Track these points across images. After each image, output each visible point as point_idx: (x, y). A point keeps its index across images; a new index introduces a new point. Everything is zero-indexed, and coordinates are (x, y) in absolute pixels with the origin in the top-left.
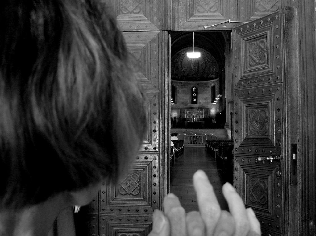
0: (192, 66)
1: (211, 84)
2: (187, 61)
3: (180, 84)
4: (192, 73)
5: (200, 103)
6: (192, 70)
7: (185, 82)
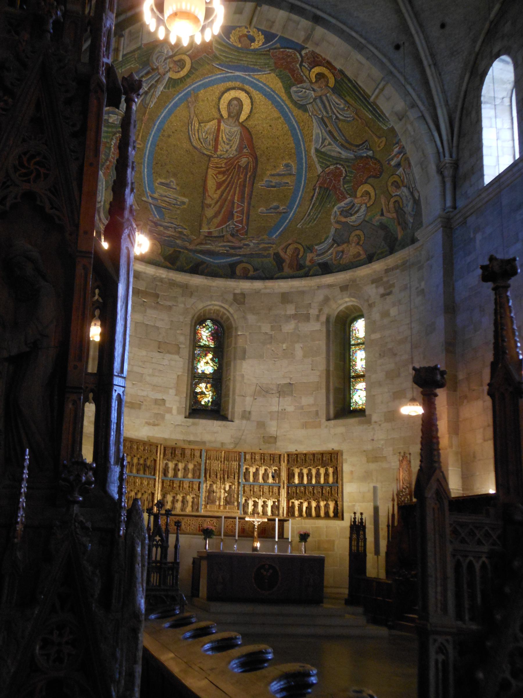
0: (211, 184)
2: (186, 145)
4: (205, 230)
5: (246, 416)
6: (210, 213)
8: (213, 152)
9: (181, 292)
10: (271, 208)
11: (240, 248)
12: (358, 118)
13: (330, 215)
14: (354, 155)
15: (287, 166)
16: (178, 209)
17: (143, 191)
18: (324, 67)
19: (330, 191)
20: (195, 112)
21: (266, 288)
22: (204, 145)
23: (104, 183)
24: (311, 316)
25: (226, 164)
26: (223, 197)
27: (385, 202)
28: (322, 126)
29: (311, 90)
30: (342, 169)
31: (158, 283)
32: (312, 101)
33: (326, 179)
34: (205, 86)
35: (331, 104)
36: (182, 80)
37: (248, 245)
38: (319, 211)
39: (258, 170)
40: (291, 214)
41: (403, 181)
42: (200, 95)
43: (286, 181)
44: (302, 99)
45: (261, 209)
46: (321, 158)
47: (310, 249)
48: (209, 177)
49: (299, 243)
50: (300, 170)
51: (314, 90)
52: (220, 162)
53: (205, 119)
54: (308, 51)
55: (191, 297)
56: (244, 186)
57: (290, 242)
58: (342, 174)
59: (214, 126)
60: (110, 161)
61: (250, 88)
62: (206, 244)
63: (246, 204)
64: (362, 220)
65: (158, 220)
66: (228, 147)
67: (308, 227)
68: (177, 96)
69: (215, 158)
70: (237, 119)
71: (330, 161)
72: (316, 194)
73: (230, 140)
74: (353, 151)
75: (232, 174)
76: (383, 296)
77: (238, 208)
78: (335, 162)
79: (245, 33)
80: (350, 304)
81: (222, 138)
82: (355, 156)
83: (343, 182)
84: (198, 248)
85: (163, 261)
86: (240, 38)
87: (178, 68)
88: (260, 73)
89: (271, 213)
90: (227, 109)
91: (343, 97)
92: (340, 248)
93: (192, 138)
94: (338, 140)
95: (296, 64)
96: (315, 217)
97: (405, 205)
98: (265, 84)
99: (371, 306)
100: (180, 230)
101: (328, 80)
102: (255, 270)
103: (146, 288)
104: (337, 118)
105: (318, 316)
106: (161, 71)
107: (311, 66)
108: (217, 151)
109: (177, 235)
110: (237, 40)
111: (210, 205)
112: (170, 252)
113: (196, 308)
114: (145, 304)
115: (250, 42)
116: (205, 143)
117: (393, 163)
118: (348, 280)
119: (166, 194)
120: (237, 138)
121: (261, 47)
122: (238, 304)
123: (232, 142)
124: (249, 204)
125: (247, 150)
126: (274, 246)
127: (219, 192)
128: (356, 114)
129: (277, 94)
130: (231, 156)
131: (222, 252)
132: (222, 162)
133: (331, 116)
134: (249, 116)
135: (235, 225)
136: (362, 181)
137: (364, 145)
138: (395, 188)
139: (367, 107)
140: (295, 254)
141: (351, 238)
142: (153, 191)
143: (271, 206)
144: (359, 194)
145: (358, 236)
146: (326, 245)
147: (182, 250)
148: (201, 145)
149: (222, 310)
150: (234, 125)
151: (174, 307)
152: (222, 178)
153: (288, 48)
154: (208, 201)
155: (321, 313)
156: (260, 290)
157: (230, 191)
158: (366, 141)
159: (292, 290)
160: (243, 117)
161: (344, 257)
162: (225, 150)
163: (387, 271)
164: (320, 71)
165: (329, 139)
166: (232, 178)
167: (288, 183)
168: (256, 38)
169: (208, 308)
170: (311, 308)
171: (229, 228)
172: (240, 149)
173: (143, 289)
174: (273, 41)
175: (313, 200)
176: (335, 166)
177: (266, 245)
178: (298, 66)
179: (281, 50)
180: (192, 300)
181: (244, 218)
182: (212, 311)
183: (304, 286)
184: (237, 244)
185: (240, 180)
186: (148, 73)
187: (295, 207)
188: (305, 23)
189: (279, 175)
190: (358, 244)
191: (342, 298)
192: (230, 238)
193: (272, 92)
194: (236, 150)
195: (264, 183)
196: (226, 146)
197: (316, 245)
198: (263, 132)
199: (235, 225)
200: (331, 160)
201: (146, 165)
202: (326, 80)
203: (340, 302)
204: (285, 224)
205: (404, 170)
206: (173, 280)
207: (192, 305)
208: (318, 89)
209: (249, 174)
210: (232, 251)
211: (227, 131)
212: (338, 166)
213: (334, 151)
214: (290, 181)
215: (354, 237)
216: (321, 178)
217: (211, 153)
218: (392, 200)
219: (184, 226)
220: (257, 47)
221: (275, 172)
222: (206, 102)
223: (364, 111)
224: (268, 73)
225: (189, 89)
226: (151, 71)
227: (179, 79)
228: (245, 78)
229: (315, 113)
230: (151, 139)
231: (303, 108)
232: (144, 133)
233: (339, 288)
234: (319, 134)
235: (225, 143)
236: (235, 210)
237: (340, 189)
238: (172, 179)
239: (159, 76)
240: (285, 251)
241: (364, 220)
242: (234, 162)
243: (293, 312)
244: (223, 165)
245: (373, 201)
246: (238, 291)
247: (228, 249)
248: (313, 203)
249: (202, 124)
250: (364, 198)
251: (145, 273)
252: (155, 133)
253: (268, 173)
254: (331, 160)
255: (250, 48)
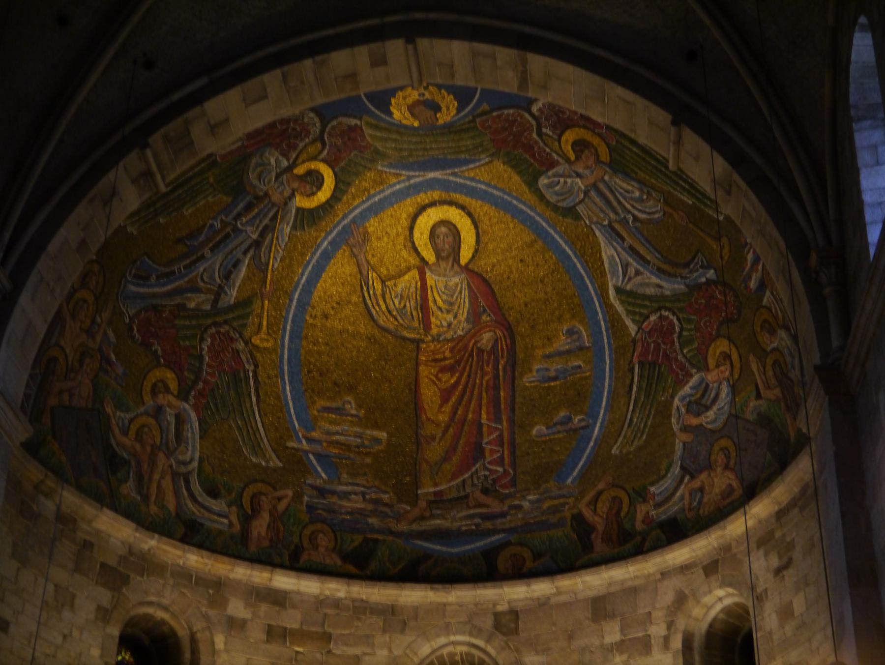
0: (429, 394)
1: (681, 599)
3: (264, 608)
4: (427, 489)
6: (434, 452)
7: (337, 589)
8: (422, 331)
9: (381, 624)
10: (555, 424)
11: (503, 515)
12: (670, 211)
13: (670, 416)
14: (685, 284)
15: (571, 332)
16: (367, 454)
17: (288, 429)
18: (580, 127)
19: (660, 367)
20: (368, 262)
21: (559, 593)
22: (401, 321)
23: (197, 425)
24: (653, 641)
25: (452, 350)
26: (457, 417)
27: (758, 369)
28: (615, 240)
29: (574, 175)
30: (671, 317)
31: (329, 611)
32: (582, 196)
33: (648, 345)
34: (376, 210)
35: (618, 195)
36: (327, 207)
37: (519, 508)
38: (647, 412)
39: (518, 350)
40: (597, 429)
41: (776, 317)
42: (371, 229)
43: (576, 364)
44: (564, 197)
45: (538, 429)
46: (629, 304)
47: (642, 495)
48: (424, 381)
49: (618, 486)
50: (596, 335)
51: (579, 175)
52: (441, 347)
53: (392, 272)
54: (541, 106)
55: (403, 631)
56: (497, 388)
57: (601, 486)
58: (674, 328)
59: (413, 282)
60: (206, 382)
61: (464, 197)
62: (432, 517)
63: (505, 423)
64: (726, 416)
65: (325, 481)
66: (450, 317)
67: (632, 449)
68: (325, 238)
69: (428, 342)
70: (454, 260)
71: (646, 307)
72: (636, 379)
73: (451, 304)
74: (682, 277)
75: (468, 368)
76: (778, 571)
77: (490, 434)
78: (655, 305)
79: (417, 97)
80: (728, 602)
81: (435, 301)
82: (687, 286)
83: (679, 343)
84: (415, 527)
85: (339, 562)
86: (411, 108)
87: (312, 188)
88: (472, 166)
89: (559, 432)
90: (430, 246)
91: (634, 175)
92: (697, 484)
93: (374, 312)
94: (648, 262)
95: (531, 134)
96: (642, 425)
97: (790, 366)
98: (488, 185)
99: (759, 599)
100: (374, 496)
101: (596, 150)
102: (537, 556)
103: (302, 623)
104: (635, 218)
105: (667, 639)
106: (276, 198)
107: (558, 132)
108: (430, 328)
109: (370, 507)
110: (407, 114)
111: (433, 438)
112: (356, 543)
113: (416, 654)
114: (300, 657)
115: (432, 113)
116: (402, 318)
117: (753, 284)
118: (715, 549)
119: (338, 428)
120: (463, 296)
121: (457, 118)
122: (504, 634)
123: (456, 307)
124: (512, 422)
125: (489, 315)
126: (571, 501)
127: (448, 408)
128: (666, 203)
129: (516, 198)
130: (460, 332)
131: (466, 531)
132: (443, 349)
133: (625, 217)
134: (476, 251)
135: (486, 469)
136: (711, 334)
137: (696, 260)
138: (767, 335)
139: (677, 184)
140: (614, 511)
141: (713, 457)
142: (309, 425)
143: (556, 419)
144: (711, 363)
145: (724, 450)
146: (670, 481)
147: (380, 537)
148: (396, 323)
149: (474, 651)
150: (452, 273)
151: (367, 658)
152: (449, 380)
153: (506, 107)
154: (429, 430)
155: (672, 630)
156: (549, 599)
157: (470, 402)
158: (698, 251)
159: (613, 589)
160: (465, 255)
161: (705, 500)
162: (445, 324)
163: (780, 514)
164: (577, 138)
165: (634, 264)
166: (469, 376)
167: (579, 367)
168: (440, 103)
169: (445, 651)
170: (651, 622)
171: (478, 478)
172: (475, 316)
173: (295, 625)
174: (475, 101)
175: (634, 392)
176: (658, 314)
177: (556, 502)
178: (535, 135)
179: (495, 114)
180: (408, 638)
181: (506, 453)
182: (458, 658)
183: (636, 577)
184: (496, 507)
185: (487, 378)
186: (249, 207)
187: (602, 412)
188: (505, 54)
189: (560, 354)
190: (727, 467)
191: (710, 592)
192: (482, 498)
193: (506, 197)
194: (467, 320)
195: (535, 374)
196: (445, 315)
197: (652, 484)
198: (512, 276)
199: (486, 469)
200: (647, 303)
201: (286, 378)
202: (593, 150)
203: (708, 600)
204: (588, 451)
205: (772, 293)
206: (362, 600)
207: (406, 648)
208: (585, 172)
209: (502, 362)
210: (488, 525)
211: (441, 286)
212: (665, 313)
213: (648, 285)
214: (584, 362)
215: (718, 454)
216: (639, 345)
217: (418, 333)
218: (769, 361)
219: (383, 487)
220: (448, 119)
221: (551, 350)
222: (385, 239)
223: (676, 193)
224: (487, 163)
225: (345, 222)
226: (255, 202)
227: (318, 208)
228: (449, 181)
229: (595, 219)
230: (288, 328)
231: (571, 212)
232: (272, 319)
233: (701, 571)
234: (613, 256)
235: (442, 311)
236: (486, 440)
237: (676, 359)
238: (348, 398)
239: (275, 210)
240: (593, 508)
241: (731, 414)
242: (466, 347)
243: (617, 637)
244: (448, 354)
245: (739, 371)
246: (502, 607)
247: (477, 520)
248: (633, 397)
249: (388, 283)
250: (723, 368)
251: (298, 593)
252: (295, 316)
253: (539, 353)
254: (647, 303)
255: (438, 124)
